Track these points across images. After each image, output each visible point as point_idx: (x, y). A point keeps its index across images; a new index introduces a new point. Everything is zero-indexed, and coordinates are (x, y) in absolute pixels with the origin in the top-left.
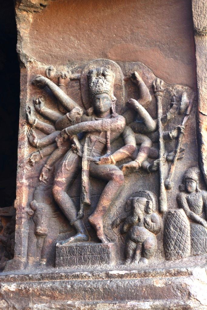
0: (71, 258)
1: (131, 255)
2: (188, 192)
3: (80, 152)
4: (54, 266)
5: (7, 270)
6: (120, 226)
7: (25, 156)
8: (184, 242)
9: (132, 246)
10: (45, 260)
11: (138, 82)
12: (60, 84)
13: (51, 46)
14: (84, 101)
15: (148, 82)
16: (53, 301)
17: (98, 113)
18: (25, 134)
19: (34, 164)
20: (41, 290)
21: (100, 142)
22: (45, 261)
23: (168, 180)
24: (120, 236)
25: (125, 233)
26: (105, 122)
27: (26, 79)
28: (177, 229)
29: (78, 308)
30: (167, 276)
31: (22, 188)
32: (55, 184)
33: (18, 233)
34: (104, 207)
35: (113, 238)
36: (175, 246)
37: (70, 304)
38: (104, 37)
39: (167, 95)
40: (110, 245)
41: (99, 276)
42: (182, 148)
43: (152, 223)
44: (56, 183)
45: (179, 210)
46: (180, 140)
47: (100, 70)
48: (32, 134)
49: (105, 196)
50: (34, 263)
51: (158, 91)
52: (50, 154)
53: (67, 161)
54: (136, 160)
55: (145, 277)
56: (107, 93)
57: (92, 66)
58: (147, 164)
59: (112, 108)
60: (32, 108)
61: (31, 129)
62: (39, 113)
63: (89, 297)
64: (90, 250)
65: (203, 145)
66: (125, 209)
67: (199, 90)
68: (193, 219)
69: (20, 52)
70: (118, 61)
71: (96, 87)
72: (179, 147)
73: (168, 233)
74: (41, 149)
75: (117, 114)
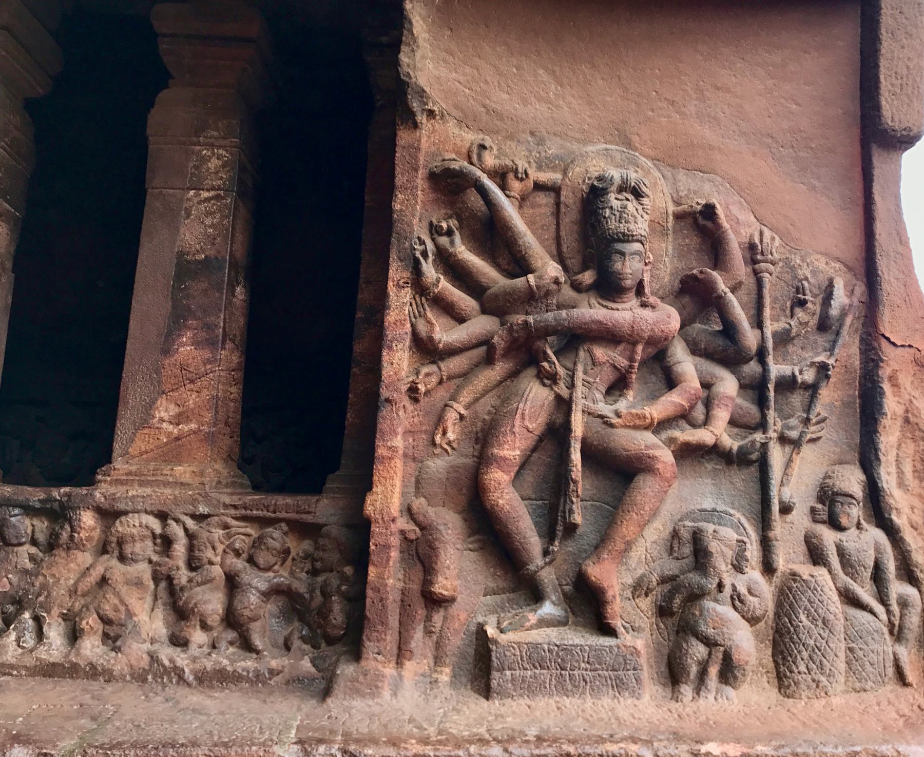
1: (692, 676)
3: (562, 385)
4: (486, 692)
5: (341, 696)
6: (654, 593)
7: (403, 373)
8: (832, 654)
9: (697, 654)
10: (447, 670)
11: (719, 226)
12: (508, 192)
13: (486, 82)
14: (565, 250)
17: (609, 288)
18: (407, 312)
19: (421, 398)
21: (615, 367)
22: (446, 674)
24: (654, 620)
25: (672, 614)
27: (416, 159)
28: (816, 620)
31: (393, 462)
32: (495, 464)
35: (637, 625)
38: (626, 90)
42: (824, 414)
43: (751, 598)
44: (497, 462)
48: (423, 315)
49: (634, 515)
51: (766, 261)
52: (465, 375)
54: (711, 429)
58: (731, 443)
59: (646, 283)
61: (423, 299)
66: (671, 550)
68: (854, 598)
69: (410, 78)
70: (657, 162)
74: (442, 359)
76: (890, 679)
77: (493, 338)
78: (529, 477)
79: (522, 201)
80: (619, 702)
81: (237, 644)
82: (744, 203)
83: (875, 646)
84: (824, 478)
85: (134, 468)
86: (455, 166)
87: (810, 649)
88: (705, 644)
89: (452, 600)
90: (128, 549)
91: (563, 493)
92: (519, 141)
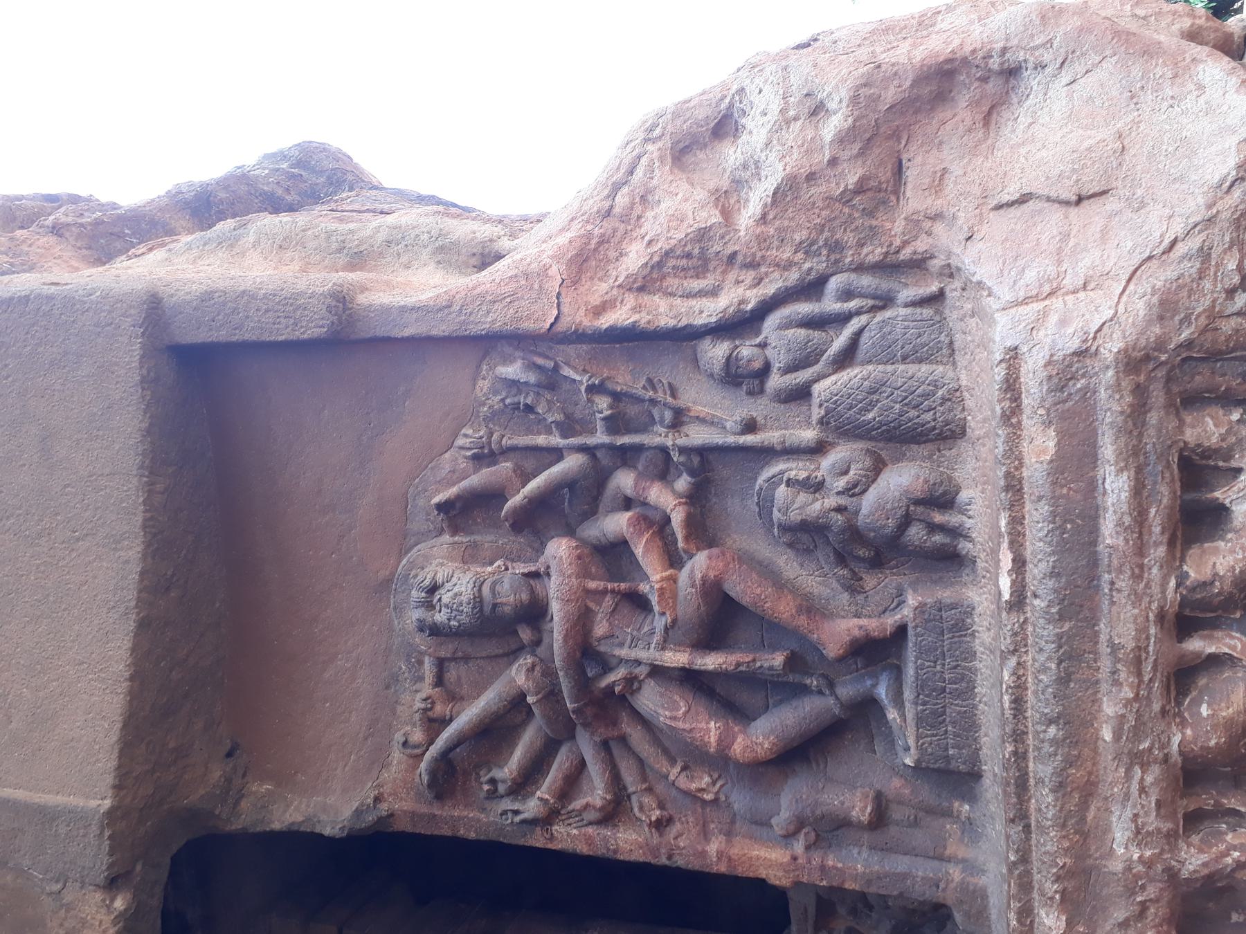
0: (954, 723)
1: (947, 540)
2: (766, 370)
3: (637, 671)
10: (956, 804)
11: (458, 497)
14: (501, 651)
15: (464, 470)
16: (1103, 790)
18: (575, 831)
20: (1064, 826)
22: (961, 806)
25: (878, 553)
29: (1125, 706)
30: (1019, 422)
33: (869, 882)
34: (799, 610)
37: (1114, 733)
40: (912, 600)
41: (1015, 634)
42: (643, 382)
43: (852, 473)
48: (580, 813)
51: (490, 443)
52: (641, 762)
53: (660, 711)
55: (1022, 488)
58: (683, 483)
59: (526, 571)
60: (507, 804)
62: (524, 783)
63: (1089, 667)
66: (808, 551)
72: (641, 392)
74: (625, 788)
75: (542, 560)
76: (937, 312)
78: (744, 697)
79: (454, 697)
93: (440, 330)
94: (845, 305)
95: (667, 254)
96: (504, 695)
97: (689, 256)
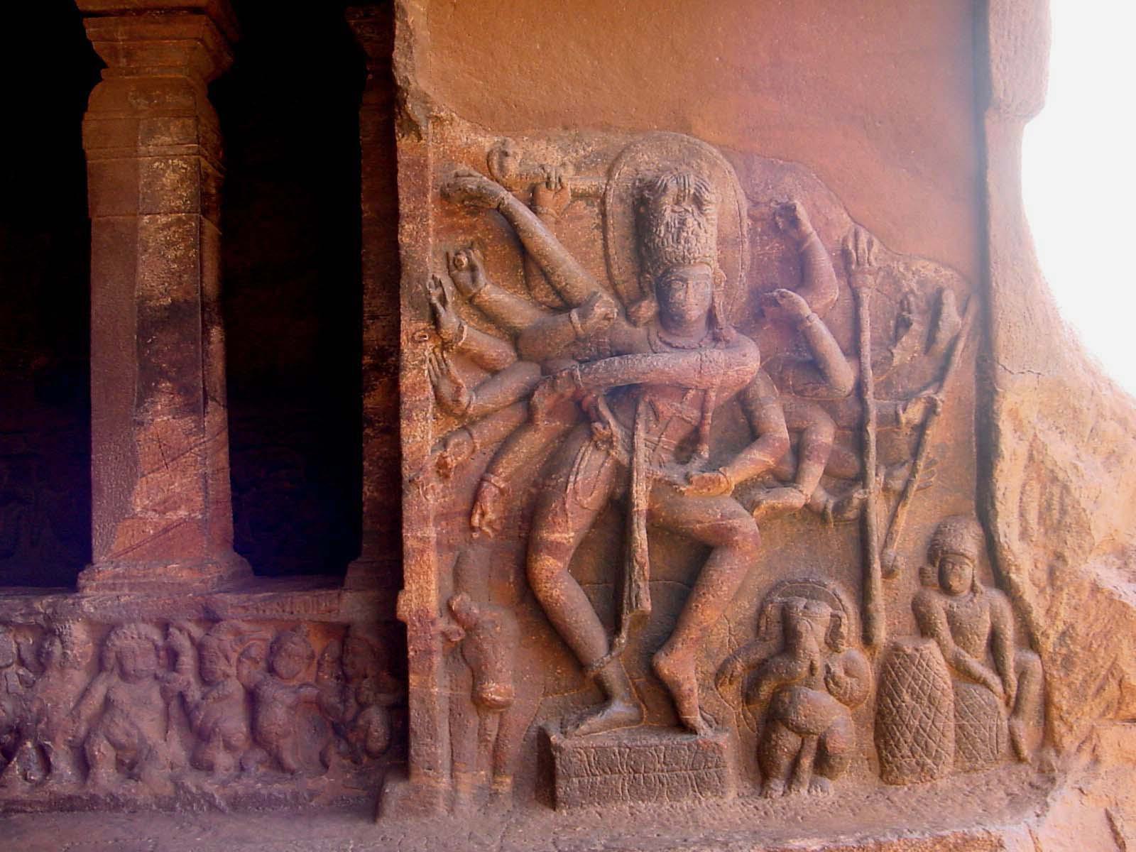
3: (620, 448)
4: (552, 801)
9: (787, 745)
10: (508, 780)
14: (616, 272)
18: (426, 372)
23: (891, 552)
24: (740, 710)
26: (711, 362)
27: (425, 180)
31: (425, 555)
33: (423, 701)
36: (913, 745)
39: (887, 287)
40: (724, 739)
43: (848, 679)
45: (927, 645)
46: (928, 435)
47: (689, 185)
48: (446, 373)
49: (711, 598)
50: (475, 791)
51: (863, 272)
56: (708, 264)
57: (645, 156)
58: (822, 497)
62: (470, 299)
64: (665, 756)
65: (1001, 459)
67: (998, 294)
68: (965, 670)
70: (726, 149)
71: (680, 243)
73: (894, 711)
74: (473, 423)
76: (1004, 755)
77: (533, 395)
80: (700, 803)
81: (268, 764)
82: (835, 198)
83: (990, 722)
84: (936, 534)
85: (120, 570)
86: (471, 185)
87: (914, 730)
88: (796, 733)
89: (507, 705)
90: (129, 665)
91: (628, 577)
92: (549, 140)
93: (995, 230)
94: (1012, 670)
95: (1065, 488)
96: (573, 281)
97: (1063, 511)
